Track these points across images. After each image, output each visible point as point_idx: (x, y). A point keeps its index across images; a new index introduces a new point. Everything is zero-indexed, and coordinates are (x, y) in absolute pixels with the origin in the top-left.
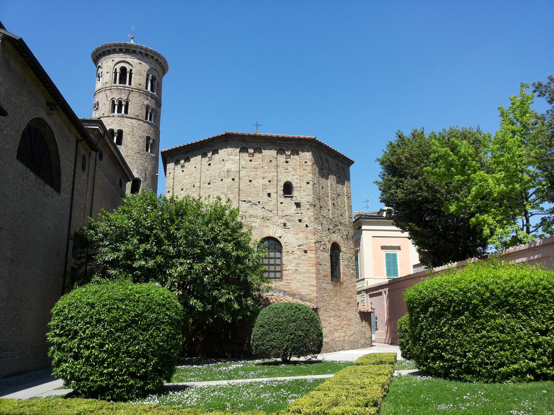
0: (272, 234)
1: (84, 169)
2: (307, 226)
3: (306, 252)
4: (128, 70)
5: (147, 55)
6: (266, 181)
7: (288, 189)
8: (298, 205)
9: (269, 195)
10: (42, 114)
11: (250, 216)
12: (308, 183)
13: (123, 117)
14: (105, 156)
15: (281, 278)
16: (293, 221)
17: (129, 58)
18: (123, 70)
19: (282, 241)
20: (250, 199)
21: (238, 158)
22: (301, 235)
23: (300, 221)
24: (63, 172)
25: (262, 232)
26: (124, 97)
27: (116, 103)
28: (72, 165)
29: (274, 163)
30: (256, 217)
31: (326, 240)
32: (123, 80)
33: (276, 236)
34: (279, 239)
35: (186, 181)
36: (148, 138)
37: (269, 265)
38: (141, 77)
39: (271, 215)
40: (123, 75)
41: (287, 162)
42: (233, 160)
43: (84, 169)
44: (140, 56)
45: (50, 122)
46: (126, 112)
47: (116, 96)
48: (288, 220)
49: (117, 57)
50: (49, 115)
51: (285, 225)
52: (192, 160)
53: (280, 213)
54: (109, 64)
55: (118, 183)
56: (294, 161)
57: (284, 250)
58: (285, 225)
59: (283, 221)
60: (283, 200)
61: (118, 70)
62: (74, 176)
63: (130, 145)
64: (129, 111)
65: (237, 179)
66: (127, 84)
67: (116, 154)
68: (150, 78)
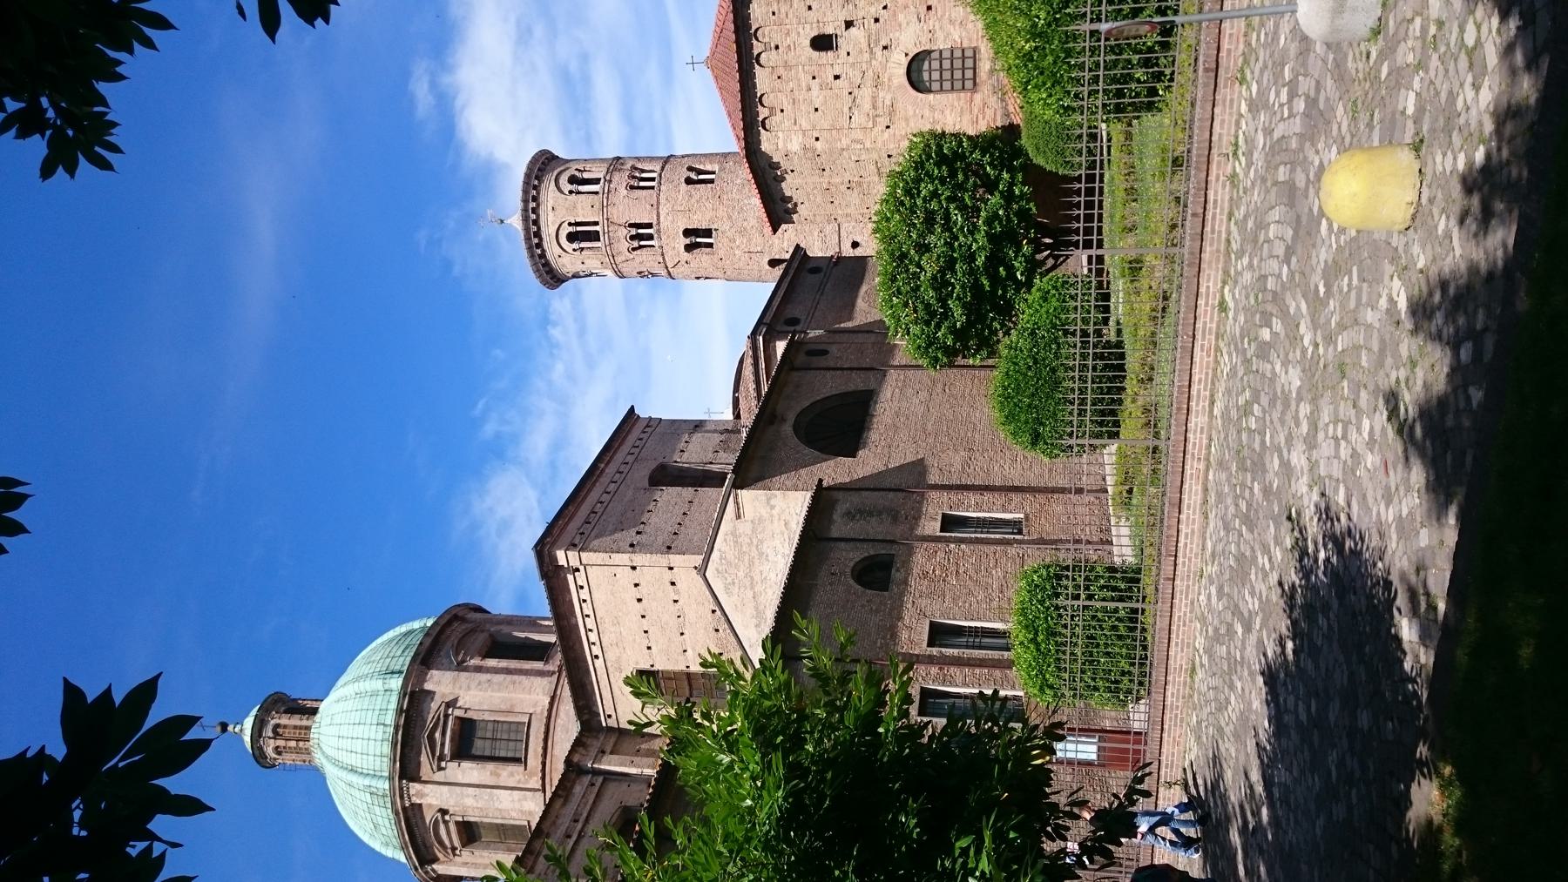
0: (903, 70)
1: (825, 352)
3: (929, 8)
4: (571, 229)
5: (535, 199)
6: (815, 84)
7: (823, 43)
8: (849, 24)
9: (837, 77)
10: (787, 429)
11: (874, 107)
13: (659, 231)
16: (877, 34)
17: (548, 231)
18: (572, 237)
19: (913, 52)
20: (846, 110)
22: (901, 17)
24: (843, 389)
25: (900, 86)
26: (623, 232)
27: (636, 244)
28: (829, 374)
29: (781, 71)
30: (874, 98)
32: (594, 236)
33: (905, 62)
35: (819, 199)
36: (689, 181)
37: (952, 69)
38: (579, 206)
40: (582, 235)
41: (777, 47)
42: (785, 141)
43: (825, 352)
44: (541, 213)
45: (791, 417)
46: (649, 226)
47: (624, 245)
48: (877, 41)
50: (784, 420)
51: (885, 48)
52: (788, 193)
54: (565, 258)
57: (927, 48)
58: (885, 48)
59: (878, 51)
60: (842, 52)
61: (575, 245)
64: (646, 221)
67: (781, 293)
68: (573, 187)
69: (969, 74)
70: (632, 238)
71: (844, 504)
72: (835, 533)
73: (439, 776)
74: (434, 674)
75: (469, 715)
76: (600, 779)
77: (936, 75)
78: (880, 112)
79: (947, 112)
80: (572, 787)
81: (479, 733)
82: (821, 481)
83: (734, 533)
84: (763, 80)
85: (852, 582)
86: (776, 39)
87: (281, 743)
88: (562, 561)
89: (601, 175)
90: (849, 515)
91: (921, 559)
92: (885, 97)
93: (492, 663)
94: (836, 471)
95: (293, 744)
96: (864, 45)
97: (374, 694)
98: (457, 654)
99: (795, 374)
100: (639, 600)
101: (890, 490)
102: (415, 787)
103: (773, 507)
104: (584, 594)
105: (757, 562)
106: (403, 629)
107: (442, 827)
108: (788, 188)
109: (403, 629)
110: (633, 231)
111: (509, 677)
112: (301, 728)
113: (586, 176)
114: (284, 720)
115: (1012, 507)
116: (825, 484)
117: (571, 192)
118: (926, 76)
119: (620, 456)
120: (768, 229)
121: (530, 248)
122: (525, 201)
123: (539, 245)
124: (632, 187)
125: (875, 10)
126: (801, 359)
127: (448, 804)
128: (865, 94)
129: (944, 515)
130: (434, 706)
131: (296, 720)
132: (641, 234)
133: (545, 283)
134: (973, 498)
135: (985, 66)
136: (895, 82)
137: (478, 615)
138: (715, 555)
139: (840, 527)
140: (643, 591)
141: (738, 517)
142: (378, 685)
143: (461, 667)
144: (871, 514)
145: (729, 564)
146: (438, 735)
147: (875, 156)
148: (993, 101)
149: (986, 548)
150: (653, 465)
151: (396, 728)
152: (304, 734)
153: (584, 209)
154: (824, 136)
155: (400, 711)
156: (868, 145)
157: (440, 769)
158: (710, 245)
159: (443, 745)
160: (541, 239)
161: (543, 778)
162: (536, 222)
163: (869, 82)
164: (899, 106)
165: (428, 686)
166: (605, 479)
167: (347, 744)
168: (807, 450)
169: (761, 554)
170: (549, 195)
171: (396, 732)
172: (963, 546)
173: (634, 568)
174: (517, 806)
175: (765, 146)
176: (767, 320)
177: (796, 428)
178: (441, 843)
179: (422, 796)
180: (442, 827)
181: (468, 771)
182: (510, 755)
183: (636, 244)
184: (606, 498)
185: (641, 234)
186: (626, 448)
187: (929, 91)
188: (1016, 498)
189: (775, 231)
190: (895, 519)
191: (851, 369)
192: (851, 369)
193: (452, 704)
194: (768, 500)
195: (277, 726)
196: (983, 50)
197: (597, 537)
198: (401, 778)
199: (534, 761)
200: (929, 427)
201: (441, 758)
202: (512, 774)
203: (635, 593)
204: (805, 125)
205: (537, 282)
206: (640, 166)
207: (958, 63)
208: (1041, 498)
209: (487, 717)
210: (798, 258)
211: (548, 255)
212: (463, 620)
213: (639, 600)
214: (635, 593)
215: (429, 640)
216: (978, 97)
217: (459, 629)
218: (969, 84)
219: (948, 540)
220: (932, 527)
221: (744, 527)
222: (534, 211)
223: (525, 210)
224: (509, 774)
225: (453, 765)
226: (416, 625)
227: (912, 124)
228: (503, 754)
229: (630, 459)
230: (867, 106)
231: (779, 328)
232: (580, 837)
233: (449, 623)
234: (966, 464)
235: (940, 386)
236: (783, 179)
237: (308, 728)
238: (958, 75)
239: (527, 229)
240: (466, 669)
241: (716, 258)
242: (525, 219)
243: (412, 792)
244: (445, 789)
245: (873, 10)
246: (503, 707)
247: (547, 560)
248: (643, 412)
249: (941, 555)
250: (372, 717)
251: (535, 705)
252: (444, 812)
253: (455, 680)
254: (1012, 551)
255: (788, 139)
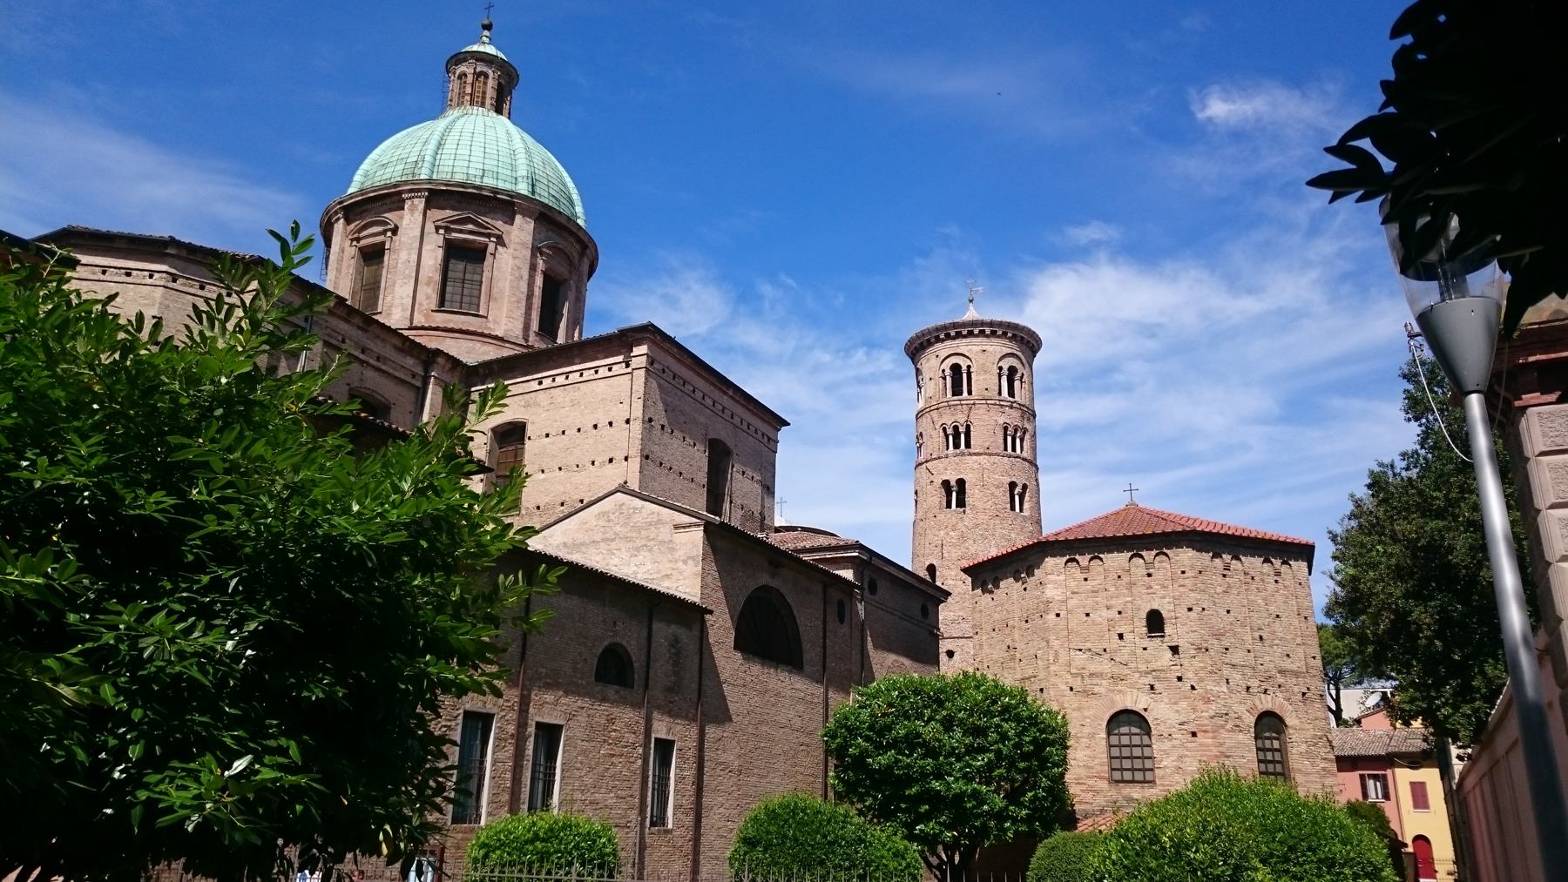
0: (1130, 706)
1: (842, 620)
2: (1193, 688)
3: (1194, 734)
4: (964, 368)
5: (993, 333)
6: (1113, 614)
7: (1155, 622)
8: (1175, 650)
9: (1121, 636)
10: (765, 579)
12: (1190, 610)
13: (963, 454)
14: (882, 585)
15: (1152, 782)
17: (963, 345)
18: (956, 368)
20: (1088, 645)
21: (1062, 577)
22: (1184, 704)
23: (1180, 679)
24: (804, 637)
25: (1113, 702)
27: (950, 431)
29: (1126, 579)
30: (1100, 675)
31: (1243, 708)
32: (957, 391)
33: (1139, 708)
34: (1145, 714)
36: (1013, 485)
37: (1132, 758)
39: (1127, 671)
40: (958, 378)
41: (1149, 575)
42: (1055, 582)
43: (842, 620)
46: (968, 445)
47: (948, 420)
48: (1157, 678)
49: (943, 349)
50: (773, 575)
51: (1152, 687)
52: (1002, 584)
53: (1143, 668)
54: (935, 362)
55: (918, 613)
56: (1162, 572)
57: (1154, 732)
58: (1152, 687)
59: (1149, 680)
60: (1146, 643)
61: (948, 372)
62: (825, 637)
63: (980, 505)
65: (1062, 614)
66: (965, 393)
67: (901, 575)
68: (1005, 371)
69: (1128, 776)
70: (956, 428)
71: (687, 637)
72: (656, 626)
73: (430, 227)
74: (530, 225)
75: (489, 258)
76: (418, 384)
77: (1125, 740)
78: (1087, 681)
79: (1088, 752)
80: (412, 356)
81: (470, 267)
82: (711, 612)
83: (659, 522)
84: (1116, 560)
85: (606, 643)
86: (1157, 575)
87: (470, 79)
88: (637, 351)
89: (1017, 398)
90: (675, 642)
91: (627, 717)
92: (1102, 687)
93: (539, 281)
94: (721, 629)
95: (469, 90)
96: (1154, 666)
97: (514, 168)
98: (548, 247)
99: (819, 588)
100: (595, 427)
101: (700, 684)
102: (420, 204)
103: (685, 562)
104: (603, 372)
105: (630, 545)
106: (576, 197)
107: (380, 229)
108: (1008, 584)
109: (576, 197)
110: (962, 429)
111: (524, 297)
112: (484, 98)
113: (1017, 384)
114: (491, 83)
115: (679, 815)
116: (708, 617)
117: (1001, 368)
118: (1124, 730)
119: (739, 410)
120: (966, 564)
121: (945, 328)
122: (991, 324)
123: (948, 337)
124: (1006, 429)
125: (1190, 677)
126: (835, 595)
127: (402, 236)
128: (1105, 666)
129: (672, 742)
130: (499, 224)
131: (491, 93)
132: (959, 437)
133: (911, 341)
134: (690, 773)
135: (1136, 792)
136: (1118, 698)
137: (586, 268)
138: (638, 503)
139: (663, 631)
140: (605, 430)
141: (676, 527)
142: (522, 171)
143: (536, 250)
144: (676, 664)
145: (629, 517)
146: (470, 227)
147: (1042, 675)
148: (1101, 800)
149: (637, 787)
150: (730, 443)
151: (479, 188)
152: (477, 100)
153: (984, 381)
154: (1061, 622)
155: (495, 191)
156: (1053, 668)
157: (437, 228)
158: (949, 506)
159: (461, 231)
160: (954, 338)
161: (423, 328)
162: (970, 334)
163: (1118, 670)
164: (1093, 702)
165: (518, 218)
166: (717, 395)
167: (465, 141)
168: (742, 600)
169: (638, 549)
170: (997, 347)
171: (475, 187)
172: (640, 762)
173: (628, 422)
174: (397, 302)
175: (1050, 562)
176: (875, 561)
177: (765, 589)
178: (365, 227)
179: (412, 210)
180: (380, 229)
181: (433, 255)
182: (448, 296)
183: (950, 431)
184: (699, 395)
185: (959, 437)
186: (748, 417)
187: (1109, 733)
188: (689, 820)
189: (965, 570)
190: (670, 690)
191: (824, 647)
192: (824, 647)
193: (500, 241)
194: (693, 558)
195: (486, 76)
196: (1154, 791)
197: (660, 386)
198: (430, 190)
199: (441, 319)
200: (764, 728)
201: (447, 230)
202: (428, 297)
203: (603, 423)
204: (1073, 602)
205: (912, 334)
206: (1027, 437)
207: (1138, 764)
208: (688, 847)
209: (486, 275)
210: (938, 594)
211: (939, 345)
212: (582, 254)
213: (595, 427)
214: (603, 423)
215: (563, 221)
216: (1104, 785)
217: (574, 250)
218: (1117, 775)
219: (646, 746)
220: (661, 730)
221: (665, 532)
222: (982, 333)
223: (983, 323)
224: (428, 296)
225: (440, 240)
226: (579, 209)
227: (1075, 714)
228: (449, 289)
229: (737, 420)
230: (1093, 668)
231: (866, 573)
232: (362, 362)
233: (579, 241)
234: (726, 767)
235: (807, 740)
236: (1017, 580)
237: (483, 105)
238: (1127, 764)
239: (964, 325)
240: (533, 255)
241: (936, 511)
242: (974, 324)
243: (416, 201)
244: (418, 233)
245: (1190, 675)
246: (495, 290)
247: (639, 336)
248: (783, 433)
249: (631, 738)
250: (491, 164)
251: (495, 322)
252: (395, 231)
253: (523, 244)
254: (634, 815)
255: (1057, 584)
